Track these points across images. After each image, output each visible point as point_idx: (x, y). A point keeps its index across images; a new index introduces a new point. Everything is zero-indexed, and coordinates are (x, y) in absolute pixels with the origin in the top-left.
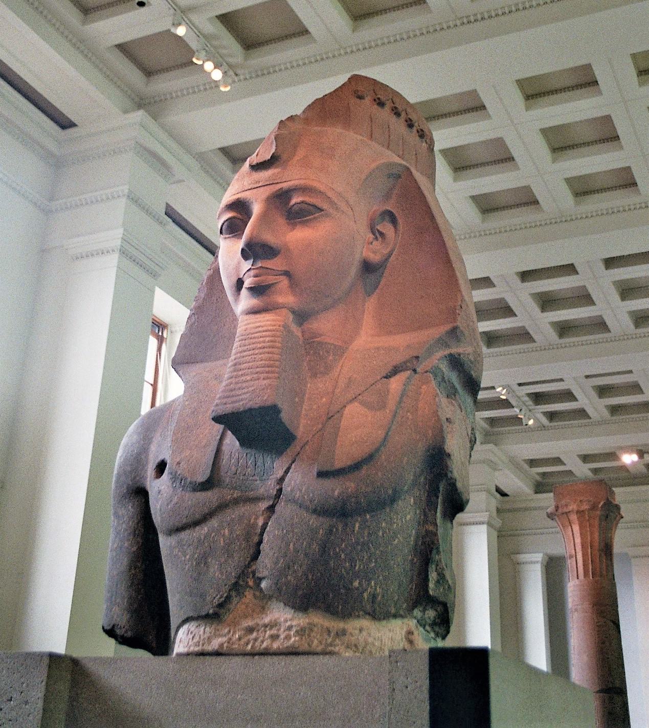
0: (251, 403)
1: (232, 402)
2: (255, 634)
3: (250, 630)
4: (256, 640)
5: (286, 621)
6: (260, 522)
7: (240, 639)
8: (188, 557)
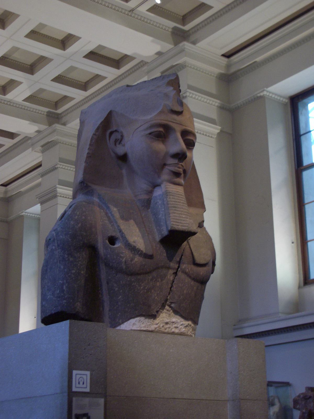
0: (190, 229)
1: (181, 226)
2: (168, 326)
3: (167, 323)
4: (169, 328)
5: (181, 321)
6: (172, 278)
7: (163, 326)
8: (142, 288)
